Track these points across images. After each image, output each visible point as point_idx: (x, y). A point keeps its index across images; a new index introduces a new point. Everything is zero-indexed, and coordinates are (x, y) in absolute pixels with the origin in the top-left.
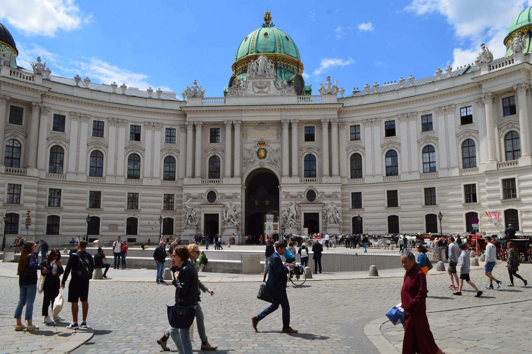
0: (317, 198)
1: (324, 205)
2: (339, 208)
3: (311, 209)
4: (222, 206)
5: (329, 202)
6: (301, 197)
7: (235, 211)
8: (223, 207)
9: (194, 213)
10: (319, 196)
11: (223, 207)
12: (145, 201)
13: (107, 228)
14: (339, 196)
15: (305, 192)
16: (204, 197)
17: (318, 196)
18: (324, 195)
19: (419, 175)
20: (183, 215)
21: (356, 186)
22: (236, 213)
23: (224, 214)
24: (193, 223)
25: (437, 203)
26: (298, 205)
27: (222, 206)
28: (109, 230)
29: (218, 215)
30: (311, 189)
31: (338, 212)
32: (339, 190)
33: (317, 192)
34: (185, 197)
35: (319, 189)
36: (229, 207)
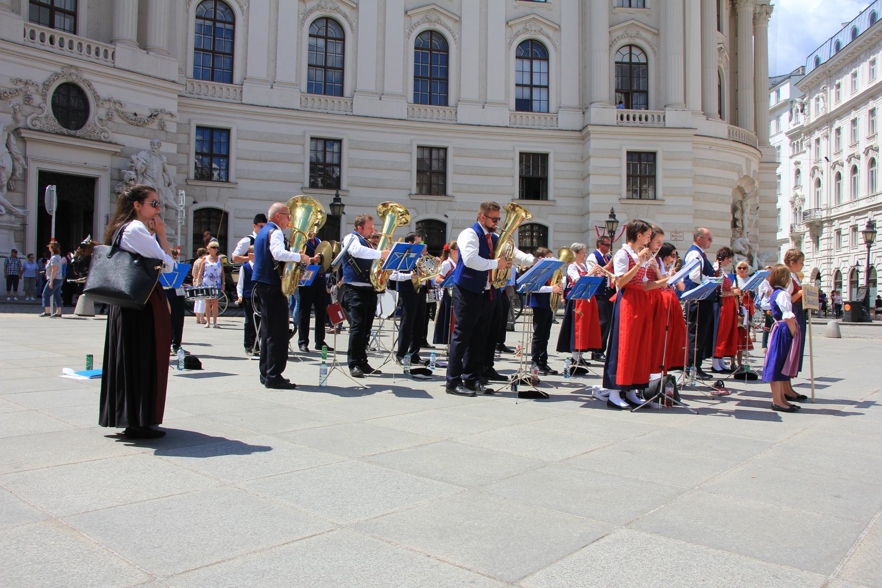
0: (93, 118)
1: (124, 154)
2: (172, 170)
3: (71, 157)
5: (145, 144)
6: (28, 99)
10: (102, 113)
14: (172, 127)
15: (46, 85)
17: (96, 113)
18: (124, 116)
19: (405, 105)
21: (214, 107)
25: (449, 191)
26: (17, 131)
30: (73, 79)
31: (169, 185)
32: (170, 104)
33: (97, 97)
35: (101, 86)
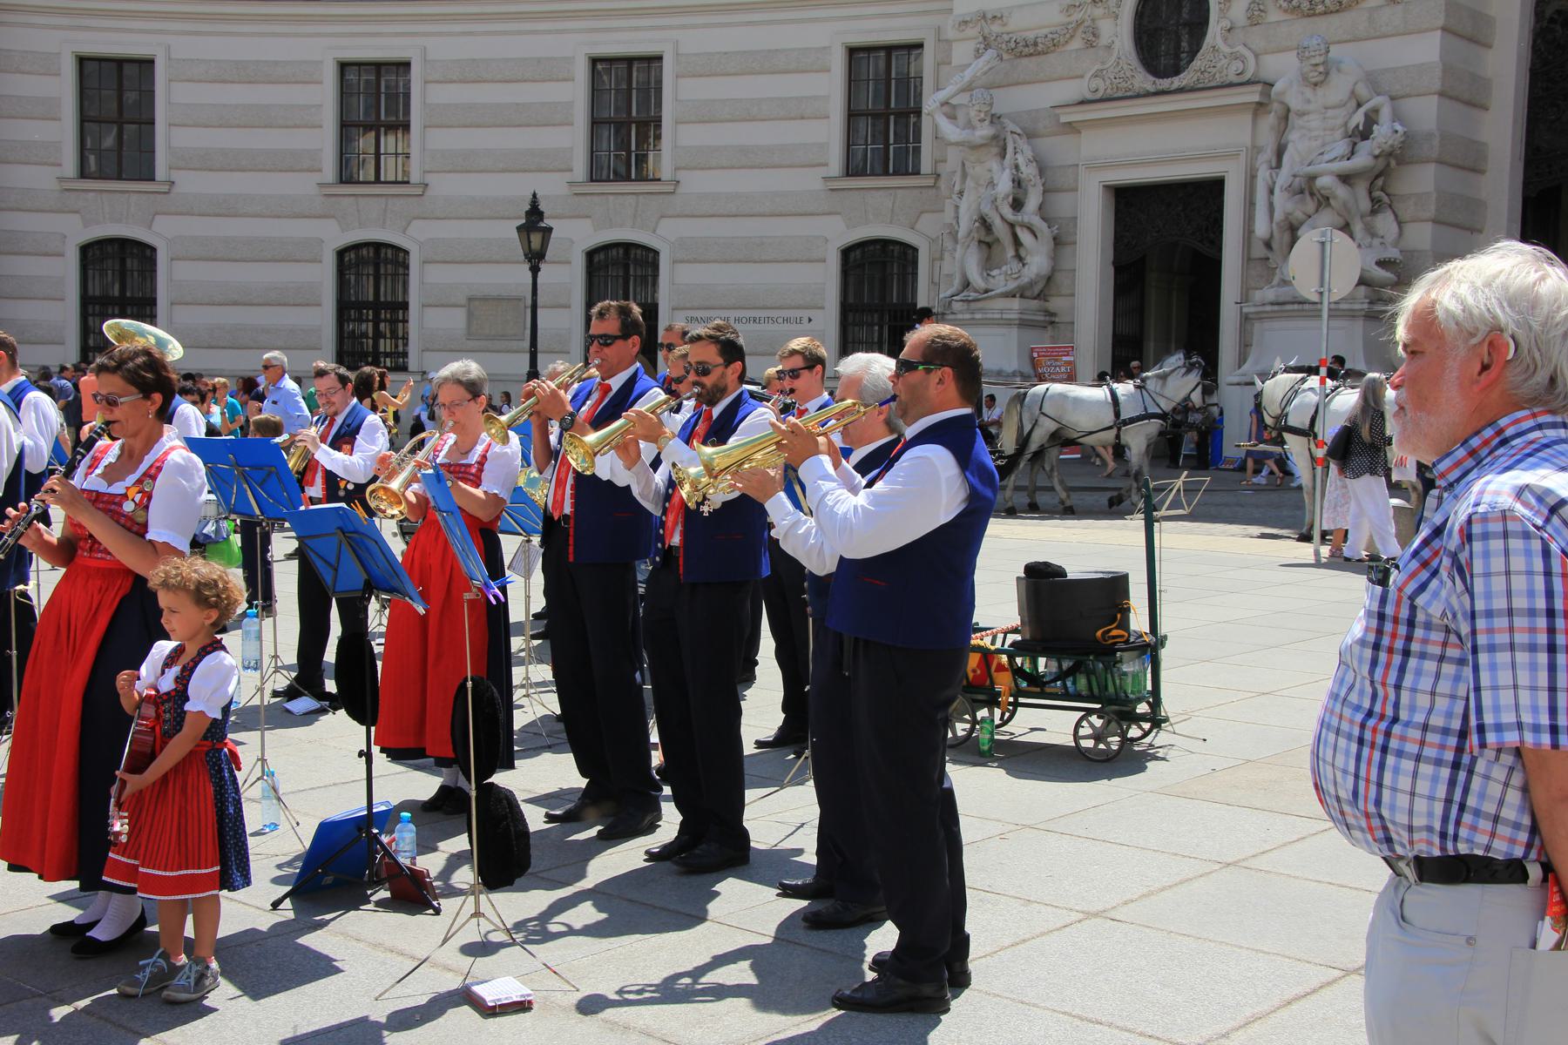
4: (1252, 95)
7: (1365, 134)
8: (1260, 108)
9: (1004, 185)
11: (1260, 108)
12: (706, 115)
13: (456, 320)
16: (1106, 28)
20: (948, 216)
22: (1362, 160)
23: (1263, 175)
24: (1001, 281)
27: (1252, 95)
28: (470, 335)
29: (1212, 189)
34: (962, 52)
36: (1295, 103)
